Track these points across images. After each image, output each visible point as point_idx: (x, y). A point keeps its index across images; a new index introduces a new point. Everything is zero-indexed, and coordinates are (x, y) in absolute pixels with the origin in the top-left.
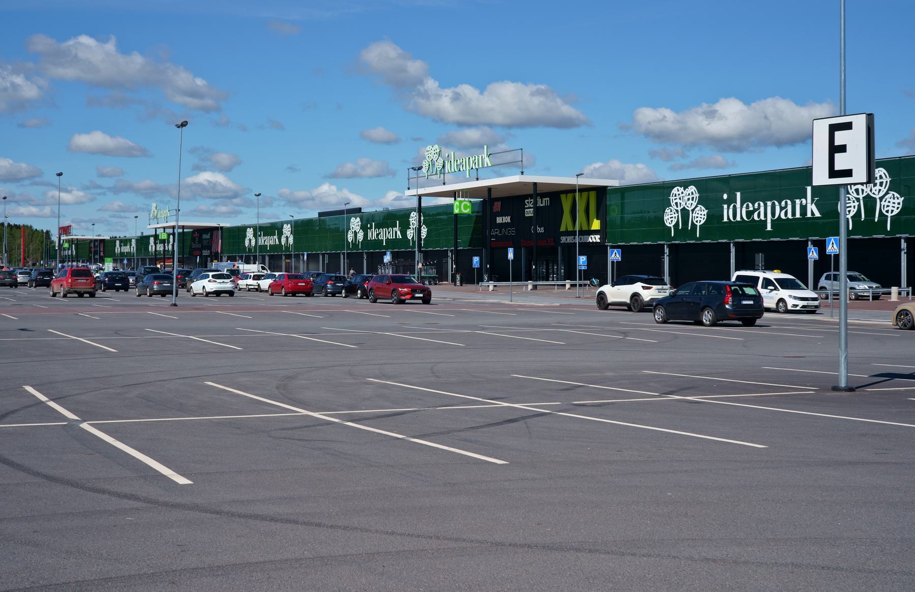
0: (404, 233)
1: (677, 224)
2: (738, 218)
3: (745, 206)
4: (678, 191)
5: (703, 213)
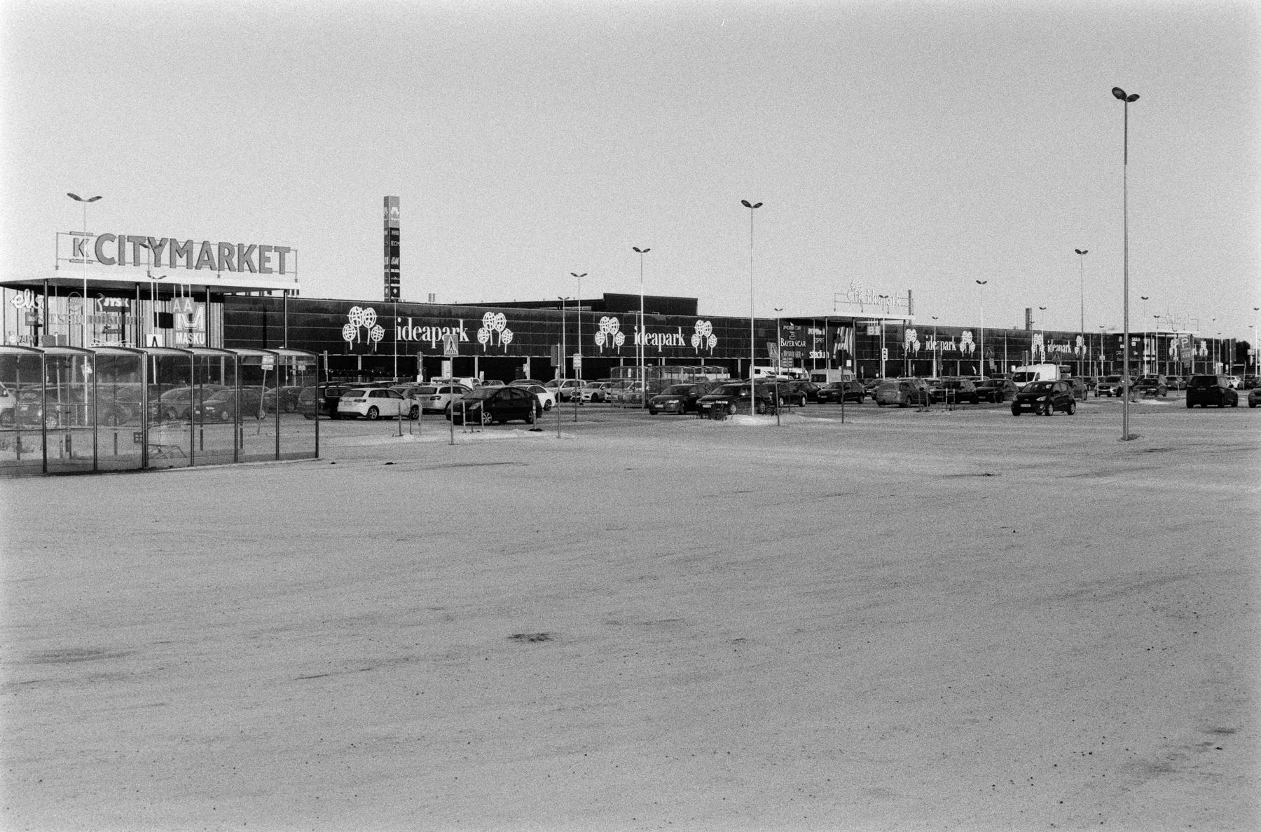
0: (688, 341)
1: (605, 344)
2: (410, 338)
3: (415, 329)
4: (357, 310)
5: (510, 335)
